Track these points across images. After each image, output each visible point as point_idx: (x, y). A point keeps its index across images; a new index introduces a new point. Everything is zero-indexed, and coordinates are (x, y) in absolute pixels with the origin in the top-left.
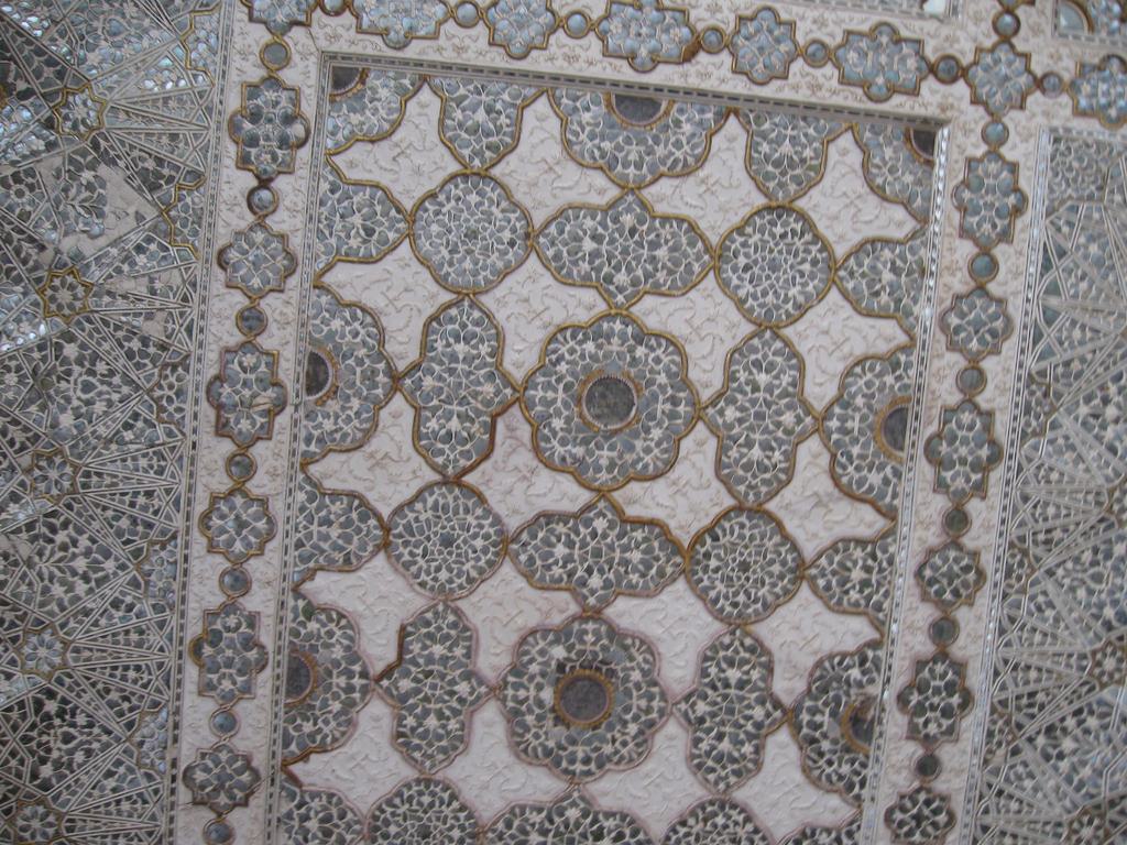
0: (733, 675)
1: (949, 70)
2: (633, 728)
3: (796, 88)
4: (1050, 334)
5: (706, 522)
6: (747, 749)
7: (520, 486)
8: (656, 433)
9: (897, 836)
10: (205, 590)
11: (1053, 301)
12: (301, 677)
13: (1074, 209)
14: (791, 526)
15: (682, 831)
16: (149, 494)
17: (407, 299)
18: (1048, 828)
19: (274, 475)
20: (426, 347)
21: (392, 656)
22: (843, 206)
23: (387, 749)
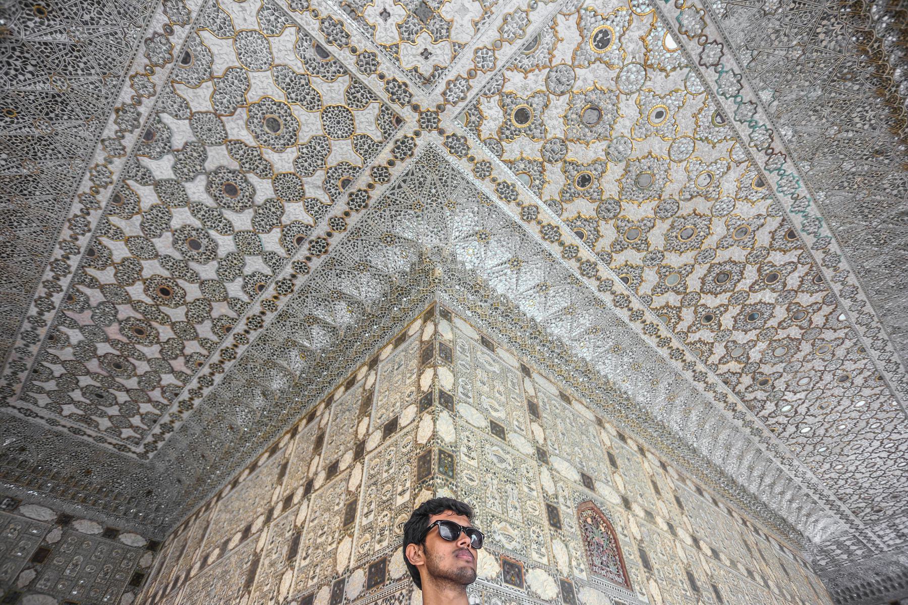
0: (273, 209)
1: (416, 108)
2: (241, 204)
3: (369, 82)
4: (396, 191)
6: (268, 227)
7: (237, 128)
10: (126, 95)
11: (402, 184)
12: (149, 135)
13: (423, 167)
14: (306, 187)
16: (114, 60)
17: (225, 56)
19: (160, 79)
20: (225, 74)
21: (180, 147)
22: (366, 121)
23: (169, 168)
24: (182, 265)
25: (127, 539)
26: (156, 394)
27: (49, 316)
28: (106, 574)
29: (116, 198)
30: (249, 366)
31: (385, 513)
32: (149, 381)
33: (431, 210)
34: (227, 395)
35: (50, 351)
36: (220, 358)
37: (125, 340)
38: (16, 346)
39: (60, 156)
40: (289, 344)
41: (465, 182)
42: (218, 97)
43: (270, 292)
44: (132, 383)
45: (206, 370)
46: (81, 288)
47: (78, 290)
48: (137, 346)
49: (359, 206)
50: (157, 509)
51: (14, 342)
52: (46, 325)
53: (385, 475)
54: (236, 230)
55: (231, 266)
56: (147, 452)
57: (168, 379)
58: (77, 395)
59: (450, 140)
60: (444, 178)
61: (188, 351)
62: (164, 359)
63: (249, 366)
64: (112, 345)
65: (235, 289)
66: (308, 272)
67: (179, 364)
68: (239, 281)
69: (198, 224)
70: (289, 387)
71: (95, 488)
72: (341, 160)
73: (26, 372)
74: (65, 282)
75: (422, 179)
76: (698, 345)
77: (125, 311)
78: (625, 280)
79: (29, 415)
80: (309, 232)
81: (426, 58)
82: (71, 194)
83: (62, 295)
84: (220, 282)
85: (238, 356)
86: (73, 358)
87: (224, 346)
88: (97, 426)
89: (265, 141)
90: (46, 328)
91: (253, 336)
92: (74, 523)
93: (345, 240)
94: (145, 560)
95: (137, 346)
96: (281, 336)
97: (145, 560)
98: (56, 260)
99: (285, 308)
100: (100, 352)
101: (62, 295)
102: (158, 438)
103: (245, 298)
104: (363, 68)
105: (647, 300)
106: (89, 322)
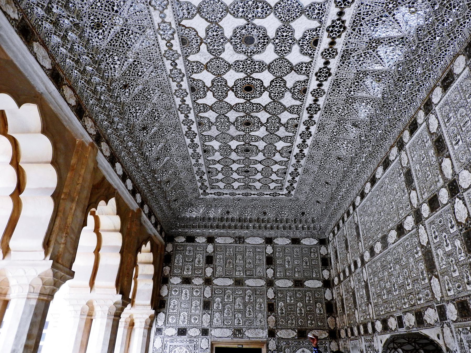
9: (337, 5)
15: (279, 5)
18: (380, 4)
24: (249, 62)
25: (306, 242)
26: (278, 157)
27: (197, 140)
28: (306, 263)
29: (183, 42)
30: (333, 110)
32: (270, 150)
34: (326, 138)
35: (209, 158)
36: (309, 115)
37: (243, 133)
38: (193, 164)
39: (138, 35)
40: (361, 76)
44: (260, 157)
45: (302, 128)
46: (201, 114)
47: (201, 117)
48: (252, 133)
50: (313, 221)
51: (191, 162)
52: (198, 146)
54: (273, 5)
55: (284, 38)
56: (289, 192)
57: (280, 145)
58: (235, 176)
61: (284, 121)
62: (271, 133)
64: (237, 140)
65: (295, 56)
67: (282, 132)
68: (296, 48)
69: (242, 22)
70: (376, 110)
71: (273, 221)
73: (205, 175)
74: (192, 116)
77: (232, 115)
79: (220, 195)
82: (160, 58)
83: (195, 124)
84: (282, 58)
85: (321, 107)
86: (221, 157)
87: (307, 105)
88: (255, 188)
90: (200, 147)
91: (326, 86)
92: (274, 241)
94: (323, 251)
95: (252, 133)
96: (350, 73)
97: (323, 251)
98: (180, 105)
99: (344, 48)
100: (233, 147)
101: (195, 124)
102: (292, 182)
103: (307, 59)
106: (217, 133)
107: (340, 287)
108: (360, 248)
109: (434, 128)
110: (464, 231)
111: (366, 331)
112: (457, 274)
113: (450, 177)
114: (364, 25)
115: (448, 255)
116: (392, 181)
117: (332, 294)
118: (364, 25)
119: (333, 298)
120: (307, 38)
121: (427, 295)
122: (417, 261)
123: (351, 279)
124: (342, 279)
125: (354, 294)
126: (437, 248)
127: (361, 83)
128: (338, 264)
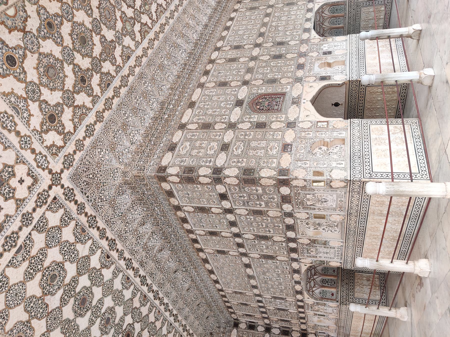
5: (76, 269)
8: (62, 272)
11: (87, 195)
14: (84, 255)
22: (54, 219)
30: (162, 282)
31: (263, 197)
33: (101, 178)
34: (174, 294)
41: (87, 157)
42: (39, 315)
43: (131, 273)
49: (95, 221)
50: (219, 327)
53: (246, 198)
54: (102, 296)
59: (66, 165)
60: (85, 169)
62: (156, 334)
63: (162, 282)
66: (123, 250)
72: (72, 234)
75: (85, 183)
76: (158, 13)
78: (129, 58)
80: (105, 251)
81: (23, 181)
89: (61, 282)
93: (110, 229)
94: (243, 326)
99: (138, 263)
104: (30, 222)
105: (138, 44)
107: (272, 319)
108: (250, 294)
109: (202, 233)
110: (258, 238)
111: (302, 307)
112: (277, 247)
113: (231, 235)
114: (135, 248)
115: (267, 248)
116: (218, 261)
117: (276, 328)
118: (135, 248)
119: (278, 328)
120: (124, 282)
121: (285, 264)
122: (267, 263)
123: (268, 308)
124: (266, 316)
125: (279, 309)
126: (263, 252)
127: (158, 260)
128: (256, 316)
